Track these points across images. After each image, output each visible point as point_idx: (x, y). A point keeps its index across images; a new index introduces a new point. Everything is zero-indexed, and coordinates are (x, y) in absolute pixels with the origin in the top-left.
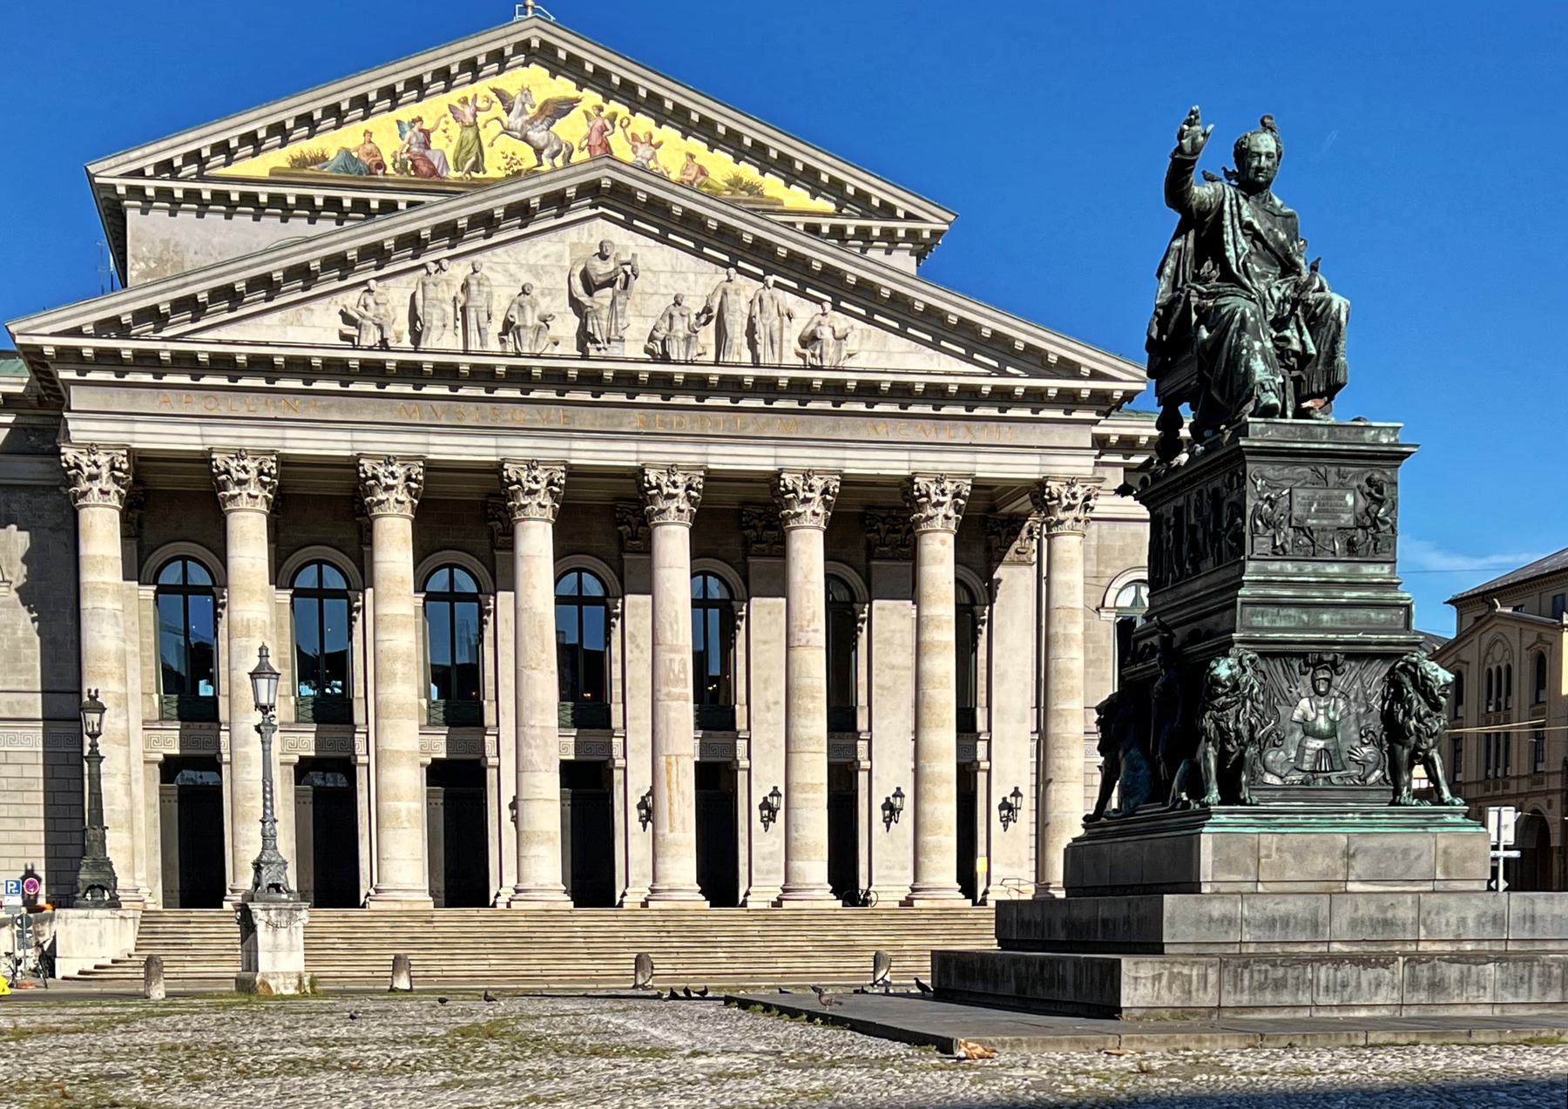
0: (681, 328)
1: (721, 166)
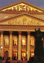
1: (35, 10)
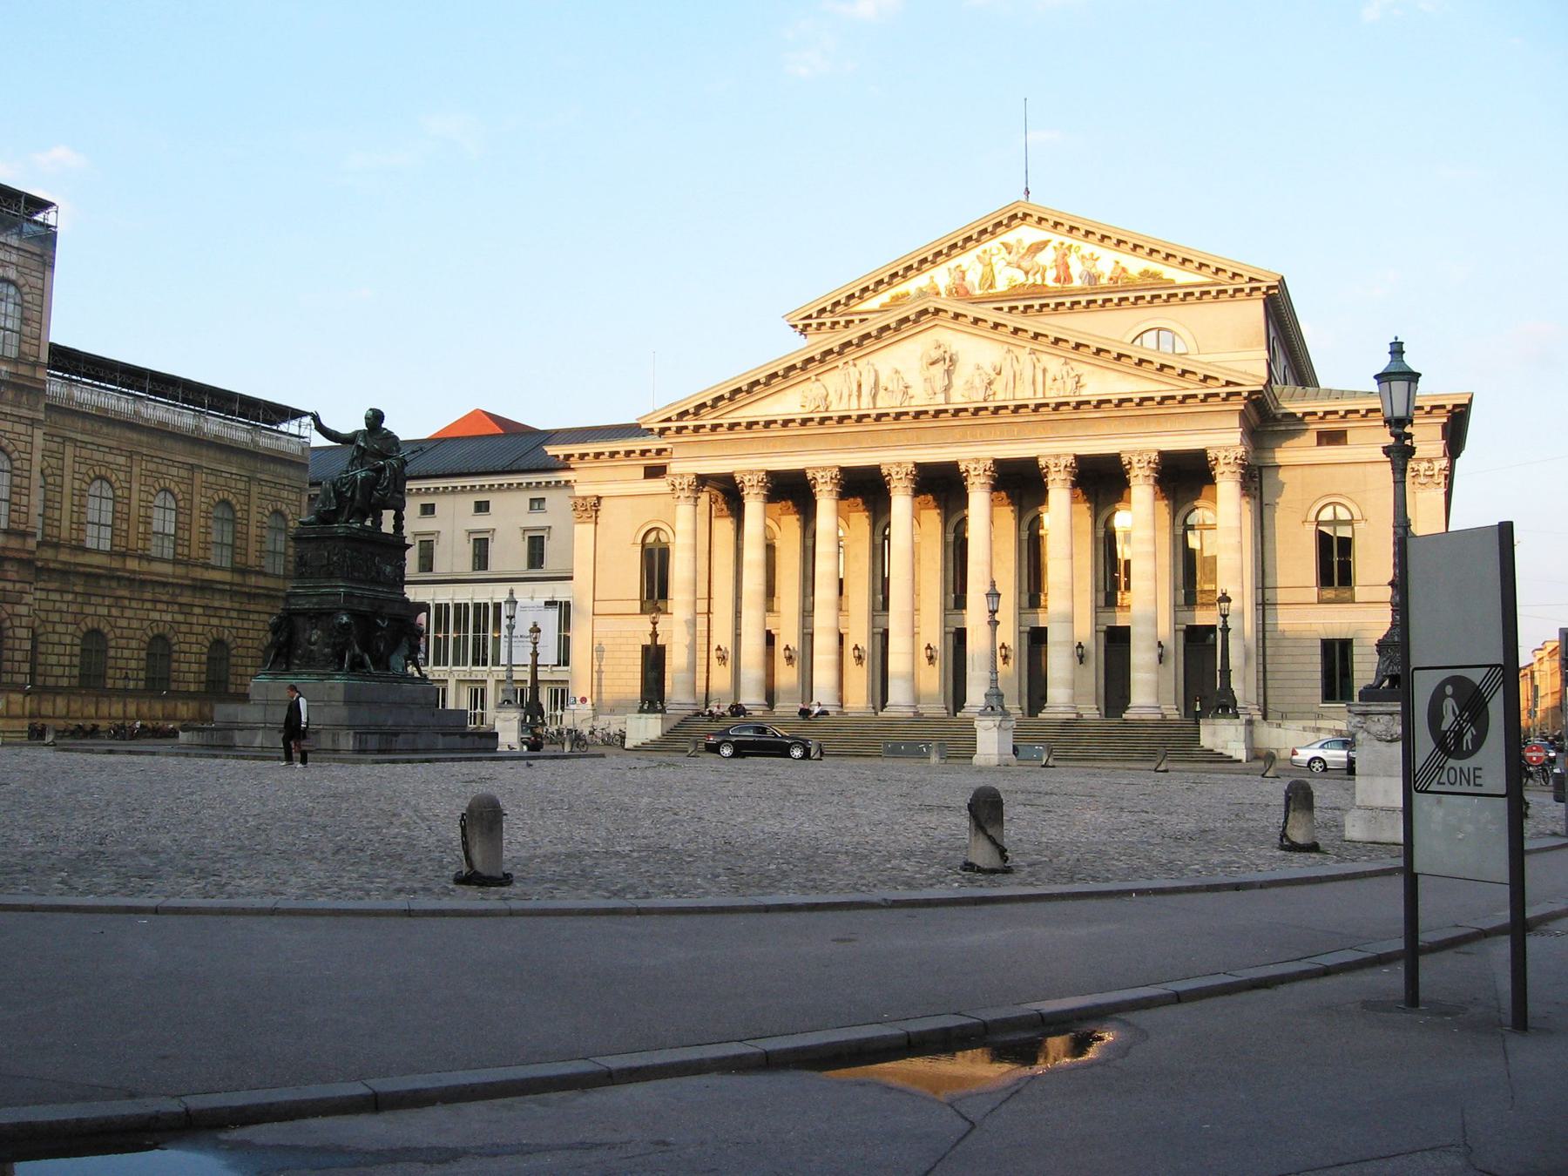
0: (977, 382)
1: (1136, 265)
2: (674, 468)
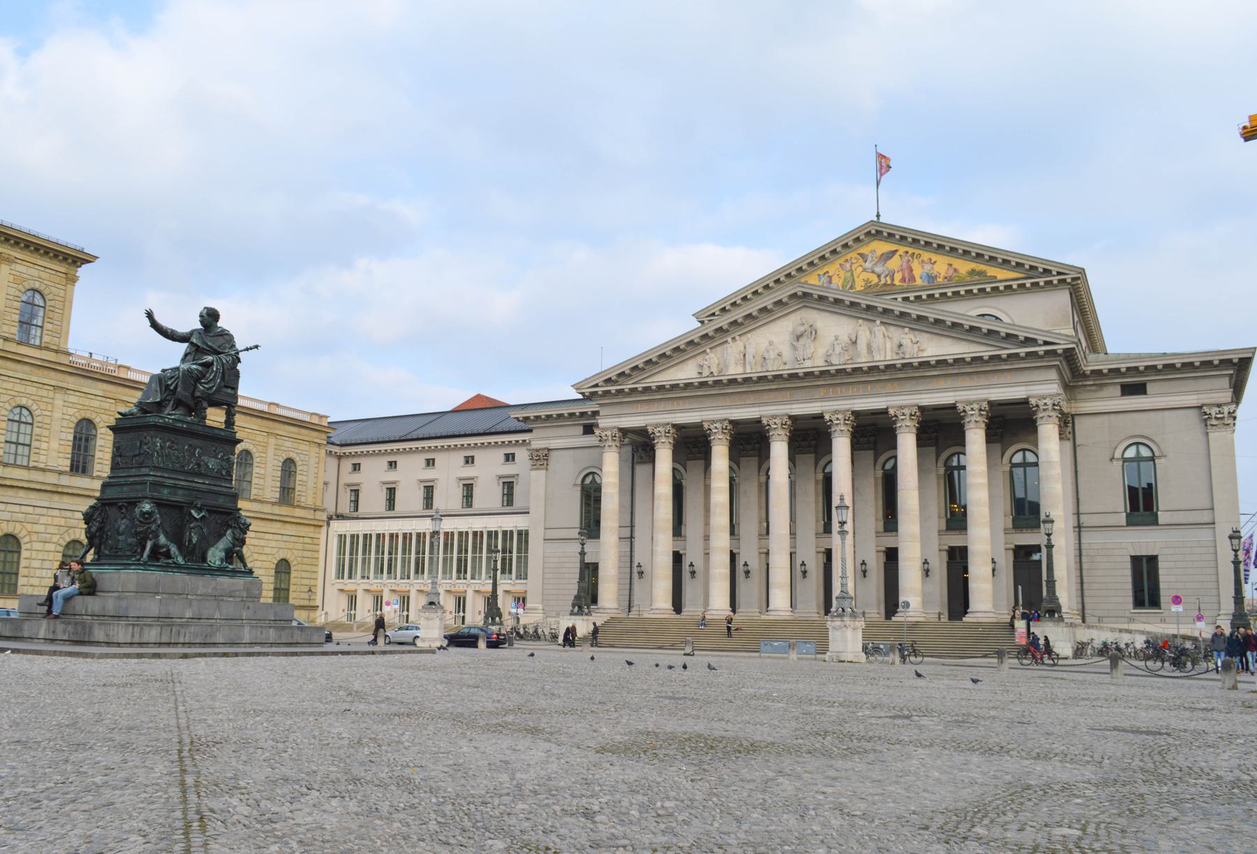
0: (838, 349)
1: (964, 267)
2: (602, 422)
